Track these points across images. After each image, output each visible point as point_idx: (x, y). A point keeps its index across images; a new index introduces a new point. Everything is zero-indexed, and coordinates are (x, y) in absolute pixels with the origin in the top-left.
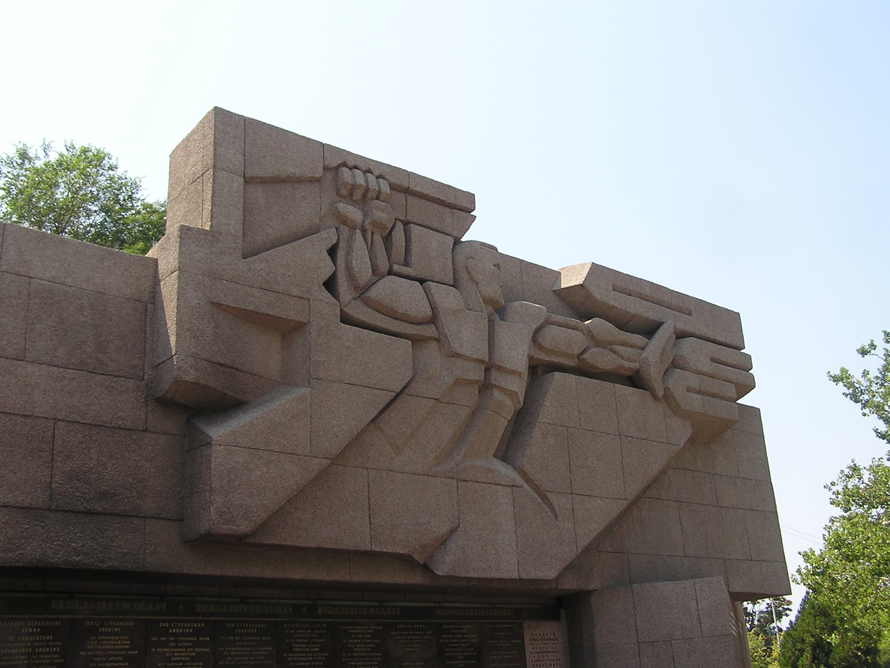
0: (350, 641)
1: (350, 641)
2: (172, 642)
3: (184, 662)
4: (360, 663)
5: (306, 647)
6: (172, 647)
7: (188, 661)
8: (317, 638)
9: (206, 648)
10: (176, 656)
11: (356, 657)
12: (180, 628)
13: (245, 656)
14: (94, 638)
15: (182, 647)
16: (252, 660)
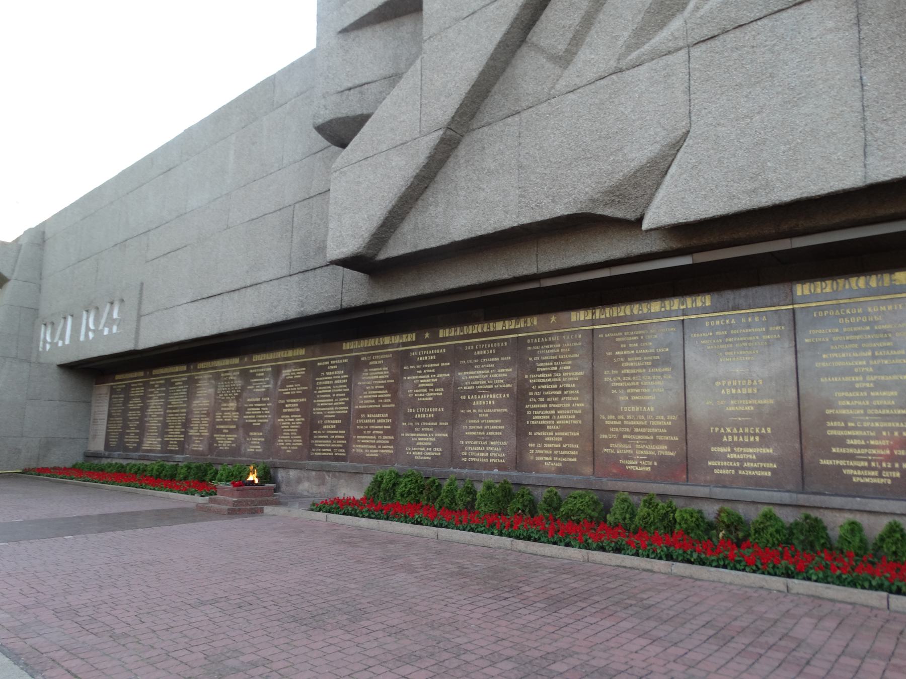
0: (618, 353)
1: (618, 353)
2: (419, 369)
3: (428, 388)
4: (633, 384)
5: (554, 366)
6: (419, 374)
7: (431, 387)
8: (568, 353)
9: (447, 373)
10: (423, 383)
11: (626, 375)
12: (426, 355)
13: (483, 379)
14: (366, 370)
15: (427, 374)
16: (490, 384)
